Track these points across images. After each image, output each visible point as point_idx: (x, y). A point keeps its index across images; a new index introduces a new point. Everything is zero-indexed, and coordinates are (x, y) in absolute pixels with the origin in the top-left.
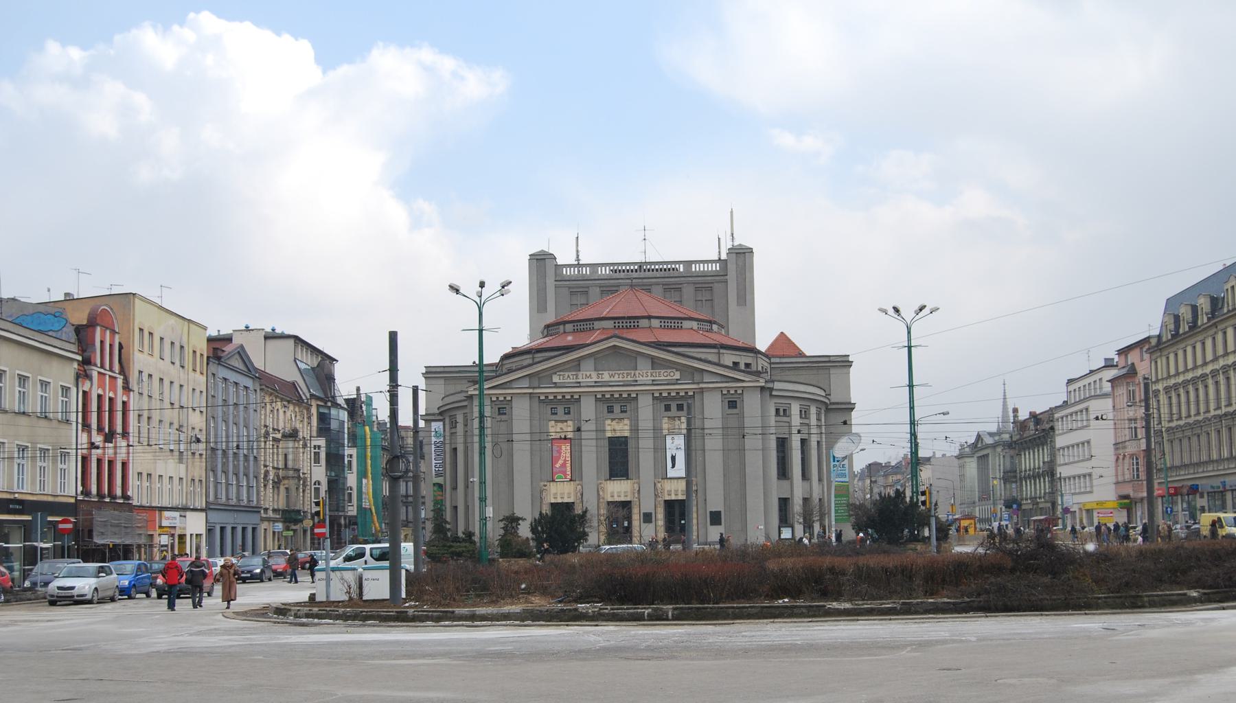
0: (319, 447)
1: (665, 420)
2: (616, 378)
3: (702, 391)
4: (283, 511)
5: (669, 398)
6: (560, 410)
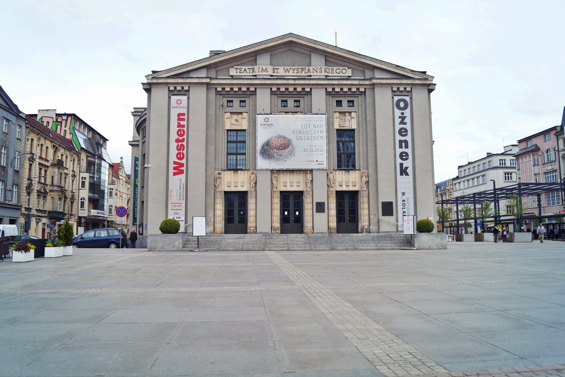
0: (85, 178)
1: (337, 114)
2: (291, 73)
3: (373, 85)
4: (50, 212)
5: (342, 93)
6: (236, 102)
